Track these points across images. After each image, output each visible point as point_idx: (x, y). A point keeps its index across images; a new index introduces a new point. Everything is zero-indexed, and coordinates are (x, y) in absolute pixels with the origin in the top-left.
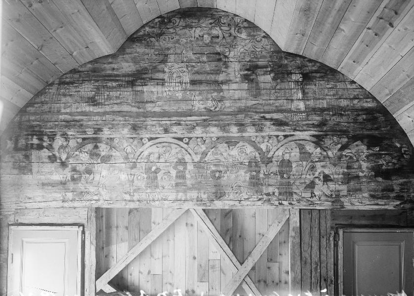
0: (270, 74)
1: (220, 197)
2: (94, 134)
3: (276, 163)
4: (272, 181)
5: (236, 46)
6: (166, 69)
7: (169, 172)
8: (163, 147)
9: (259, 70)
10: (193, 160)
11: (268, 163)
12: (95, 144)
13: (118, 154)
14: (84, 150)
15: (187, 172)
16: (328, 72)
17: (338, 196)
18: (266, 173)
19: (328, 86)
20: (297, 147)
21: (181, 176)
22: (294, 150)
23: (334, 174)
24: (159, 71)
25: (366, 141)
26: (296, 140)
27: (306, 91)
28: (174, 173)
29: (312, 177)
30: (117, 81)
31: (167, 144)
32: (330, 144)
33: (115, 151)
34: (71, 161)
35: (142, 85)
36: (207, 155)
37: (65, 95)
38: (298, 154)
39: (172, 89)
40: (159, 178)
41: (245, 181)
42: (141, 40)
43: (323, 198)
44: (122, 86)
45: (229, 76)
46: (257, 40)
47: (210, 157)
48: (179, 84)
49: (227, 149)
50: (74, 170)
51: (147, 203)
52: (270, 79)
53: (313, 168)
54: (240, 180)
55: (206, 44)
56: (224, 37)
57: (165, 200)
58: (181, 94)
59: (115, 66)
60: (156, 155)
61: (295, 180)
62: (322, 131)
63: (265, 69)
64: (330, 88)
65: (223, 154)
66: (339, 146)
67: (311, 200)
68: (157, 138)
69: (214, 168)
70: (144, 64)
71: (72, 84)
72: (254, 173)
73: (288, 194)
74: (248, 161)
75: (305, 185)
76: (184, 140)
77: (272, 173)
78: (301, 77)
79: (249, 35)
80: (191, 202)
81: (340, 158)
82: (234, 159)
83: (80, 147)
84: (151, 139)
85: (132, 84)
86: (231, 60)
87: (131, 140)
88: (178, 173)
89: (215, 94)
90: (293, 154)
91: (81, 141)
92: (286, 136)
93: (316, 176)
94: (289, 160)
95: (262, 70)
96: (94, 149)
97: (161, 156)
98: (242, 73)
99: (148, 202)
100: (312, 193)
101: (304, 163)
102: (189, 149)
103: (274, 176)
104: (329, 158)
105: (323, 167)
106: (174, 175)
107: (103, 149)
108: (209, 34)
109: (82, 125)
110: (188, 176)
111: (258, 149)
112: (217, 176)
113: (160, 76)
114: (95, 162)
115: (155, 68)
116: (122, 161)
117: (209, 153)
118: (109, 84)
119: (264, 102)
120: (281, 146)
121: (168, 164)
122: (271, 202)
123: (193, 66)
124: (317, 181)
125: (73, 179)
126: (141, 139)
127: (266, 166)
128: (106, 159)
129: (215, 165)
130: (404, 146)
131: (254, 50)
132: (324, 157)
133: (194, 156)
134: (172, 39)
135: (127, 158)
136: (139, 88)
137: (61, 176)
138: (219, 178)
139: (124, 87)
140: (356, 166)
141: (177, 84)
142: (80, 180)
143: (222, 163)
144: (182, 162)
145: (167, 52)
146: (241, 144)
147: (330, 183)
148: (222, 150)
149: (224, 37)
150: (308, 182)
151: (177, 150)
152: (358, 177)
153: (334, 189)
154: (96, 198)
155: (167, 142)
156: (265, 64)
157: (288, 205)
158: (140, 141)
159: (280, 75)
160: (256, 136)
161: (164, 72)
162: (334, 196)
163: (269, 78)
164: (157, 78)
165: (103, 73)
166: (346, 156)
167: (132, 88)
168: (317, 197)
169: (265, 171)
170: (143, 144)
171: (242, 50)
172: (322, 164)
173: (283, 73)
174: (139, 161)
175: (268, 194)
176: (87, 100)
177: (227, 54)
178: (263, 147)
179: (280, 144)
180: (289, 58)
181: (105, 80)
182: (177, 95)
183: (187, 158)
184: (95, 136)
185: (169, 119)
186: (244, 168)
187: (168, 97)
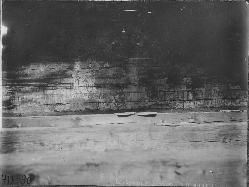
6: (73, 75)
27: (196, 92)
30: (30, 85)
35: (53, 89)
39: (79, 93)
44: (34, 90)
45: (130, 79)
48: (85, 87)
52: (165, 83)
85: (43, 88)
86: (131, 65)
89: (118, 96)
98: (140, 77)
113: (69, 80)
119: (160, 103)
136: (49, 92)
139: (36, 91)
141: (83, 88)
167: (44, 92)
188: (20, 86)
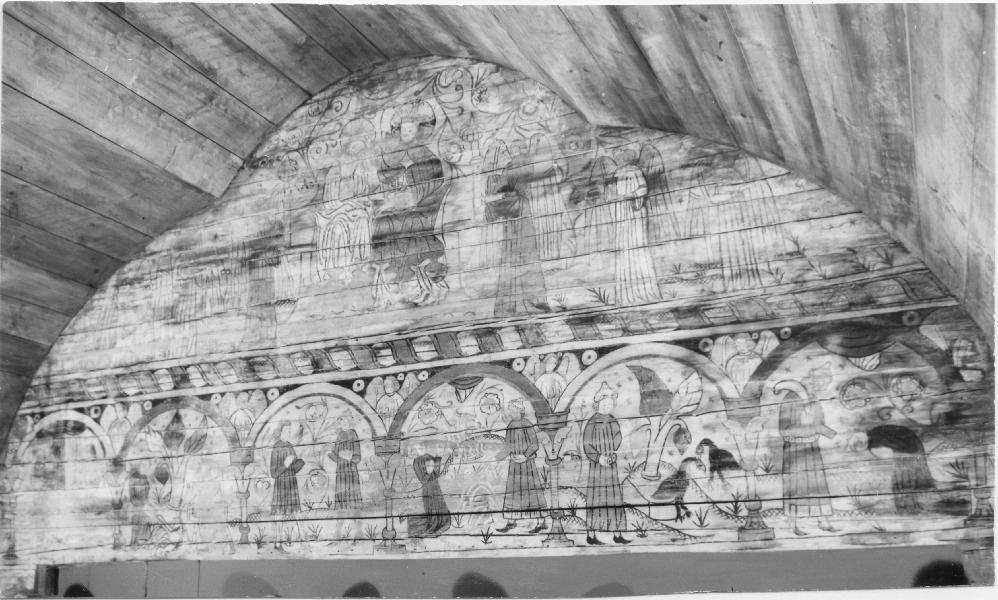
0: (559, 191)
1: (438, 527)
2: (175, 388)
3: (576, 426)
5: (476, 137)
6: (322, 222)
7: (322, 469)
8: (311, 405)
9: (533, 184)
10: (374, 433)
11: (556, 429)
12: (175, 411)
13: (218, 431)
14: (155, 428)
15: (360, 466)
16: (716, 161)
17: (754, 512)
18: (552, 457)
19: (716, 199)
21: (348, 474)
22: (627, 385)
23: (741, 446)
24: (305, 227)
25: (835, 340)
26: (630, 359)
28: (331, 468)
29: (676, 460)
31: (317, 399)
33: (214, 424)
34: (130, 454)
36: (405, 417)
37: (124, 308)
38: (636, 397)
40: (301, 484)
41: (497, 482)
42: (271, 161)
43: (712, 519)
45: (459, 211)
46: (527, 110)
47: (412, 424)
48: (347, 250)
49: (454, 398)
50: (135, 474)
51: (276, 548)
53: (680, 434)
54: (485, 479)
55: (406, 144)
56: (447, 119)
57: (315, 538)
58: (349, 274)
59: (218, 229)
60: (295, 428)
61: (632, 470)
62: (702, 327)
63: (547, 181)
64: (723, 203)
65: (444, 411)
66: (755, 363)
67: (678, 525)
68: (296, 386)
69: (421, 452)
70: (278, 214)
71: (139, 283)
72: (521, 458)
74: (505, 426)
75: (659, 483)
76: (355, 384)
77: (566, 454)
78: (640, 187)
79: (506, 101)
80: (370, 544)
81: (757, 396)
82: (470, 424)
83: (149, 417)
84: (283, 390)
85: (249, 264)
86: (466, 170)
87: (244, 396)
88: (340, 468)
90: (622, 399)
91: (150, 408)
92: (602, 352)
93: (691, 451)
94: (611, 416)
95: (541, 183)
96: (172, 422)
97: (306, 430)
99: (278, 545)
100: (679, 504)
101: (655, 421)
102: (366, 406)
103: (573, 463)
104: (725, 399)
105: (706, 427)
106: (333, 476)
107: (191, 418)
108: (413, 120)
109: (153, 371)
110: (363, 476)
111: (530, 391)
112: (428, 473)
114: (174, 453)
115: (297, 220)
116: (225, 446)
117: (412, 414)
118: (207, 271)
120: (591, 378)
121: (319, 448)
122: (569, 537)
123: (377, 203)
125: (135, 496)
126: (265, 391)
127: (552, 438)
128: (197, 443)
129: (425, 443)
130: (963, 343)
131: (517, 136)
132: (711, 400)
133: (377, 423)
134: (333, 146)
135: (234, 440)
137: (114, 490)
138: (436, 474)
140: (807, 417)
141: (342, 251)
142: (147, 497)
143: (439, 437)
144: (350, 442)
145: (321, 179)
146: (488, 381)
147: (728, 473)
148: (442, 402)
149: (447, 119)
150: (666, 474)
151: (339, 413)
152: (814, 450)
153: (743, 491)
154: (175, 537)
155: (314, 395)
156: (547, 169)
157: (614, 543)
158: (262, 395)
159: (587, 190)
160: (526, 359)
161: (315, 226)
163: (559, 200)
164: (301, 242)
165: (197, 249)
166: (777, 392)
168: (694, 518)
169: (549, 450)
170: (269, 403)
171: (490, 141)
172: (707, 419)
173: (594, 183)
174: (258, 444)
175: (557, 513)
176: (163, 314)
177: (455, 159)
178: (544, 384)
180: (608, 140)
181: (199, 264)
182: (342, 276)
183: (362, 430)
184: (175, 393)
185: (322, 337)
186: (494, 449)
187: (322, 284)
188: (200, 267)
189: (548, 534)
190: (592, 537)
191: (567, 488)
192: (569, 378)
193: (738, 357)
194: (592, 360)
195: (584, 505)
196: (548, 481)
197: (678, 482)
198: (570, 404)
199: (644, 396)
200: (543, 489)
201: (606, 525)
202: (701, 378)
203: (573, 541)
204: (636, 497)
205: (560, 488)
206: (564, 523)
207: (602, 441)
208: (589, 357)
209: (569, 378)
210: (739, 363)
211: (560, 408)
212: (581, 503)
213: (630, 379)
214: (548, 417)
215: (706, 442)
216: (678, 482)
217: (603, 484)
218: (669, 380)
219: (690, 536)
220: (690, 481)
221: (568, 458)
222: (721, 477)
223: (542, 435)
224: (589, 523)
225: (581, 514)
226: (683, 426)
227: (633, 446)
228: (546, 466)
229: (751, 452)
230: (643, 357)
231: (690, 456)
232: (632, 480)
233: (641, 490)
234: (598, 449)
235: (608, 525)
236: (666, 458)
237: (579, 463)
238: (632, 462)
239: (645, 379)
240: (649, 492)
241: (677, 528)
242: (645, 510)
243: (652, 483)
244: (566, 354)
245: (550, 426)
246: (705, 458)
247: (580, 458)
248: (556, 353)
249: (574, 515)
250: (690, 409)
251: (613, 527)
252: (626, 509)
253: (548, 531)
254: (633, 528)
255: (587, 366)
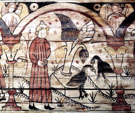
3: (25, 43)
4: (18, 71)
17: (121, 95)
18: (10, 59)
20: (58, 19)
22: (54, 24)
23: (115, 61)
26: (57, 10)
29: (80, 66)
32: (108, 17)
38: (59, 31)
43: (98, 98)
53: (83, 53)
61: (56, 69)
66: (121, 19)
73: (44, 92)
75: (70, 78)
77: (18, 59)
90: (51, 31)
94: (45, 39)
100: (81, 90)
101: (69, 44)
120: (35, 18)
122: (18, 105)
124: (88, 70)
127: (11, 48)
147: (108, 75)
150: (74, 72)
153: (114, 83)
157: (44, 109)
162: (115, 96)
168: (89, 97)
169: (9, 55)
175: (12, 92)
179: (33, 15)
189: (6, 103)
190: (32, 105)
191: (18, 77)
192: (23, 16)
193: (113, 15)
194: (35, 8)
195: (28, 87)
196: (7, 73)
197: (81, 77)
198: (22, 31)
199: (64, 30)
200: (4, 77)
201: (40, 99)
202: (94, 24)
203: (21, 107)
204: (58, 84)
205: (14, 77)
206: (16, 97)
207: (40, 53)
208: (34, 7)
209: (23, 16)
210: (114, 18)
211: (16, 32)
212: (26, 86)
213: (56, 21)
214: (9, 37)
215: (96, 57)
216: (81, 77)
217: (39, 76)
218: (77, 23)
219: (87, 107)
220: (88, 77)
221: (20, 61)
222: (104, 76)
223: (4, 47)
224: (31, 98)
225: (26, 92)
226: (85, 48)
227: (57, 57)
228: (6, 64)
229: (119, 64)
230: (64, 10)
231: (88, 64)
232: (55, 75)
233: (61, 81)
234: (37, 57)
235: (42, 99)
236: (74, 64)
237: (26, 63)
238: (56, 65)
239: (64, 21)
240: (65, 81)
241: (80, 102)
242: (63, 92)
243: (67, 77)
244: (20, 4)
245: (10, 42)
246: (96, 66)
247: (27, 61)
248: (15, 3)
249: (22, 92)
250: (88, 39)
251: (44, 100)
252: (52, 91)
253: (6, 101)
254: (56, 101)
255: (33, 12)
